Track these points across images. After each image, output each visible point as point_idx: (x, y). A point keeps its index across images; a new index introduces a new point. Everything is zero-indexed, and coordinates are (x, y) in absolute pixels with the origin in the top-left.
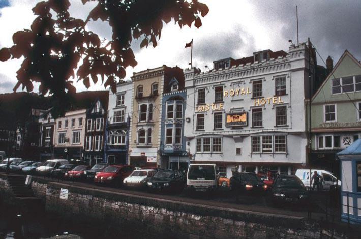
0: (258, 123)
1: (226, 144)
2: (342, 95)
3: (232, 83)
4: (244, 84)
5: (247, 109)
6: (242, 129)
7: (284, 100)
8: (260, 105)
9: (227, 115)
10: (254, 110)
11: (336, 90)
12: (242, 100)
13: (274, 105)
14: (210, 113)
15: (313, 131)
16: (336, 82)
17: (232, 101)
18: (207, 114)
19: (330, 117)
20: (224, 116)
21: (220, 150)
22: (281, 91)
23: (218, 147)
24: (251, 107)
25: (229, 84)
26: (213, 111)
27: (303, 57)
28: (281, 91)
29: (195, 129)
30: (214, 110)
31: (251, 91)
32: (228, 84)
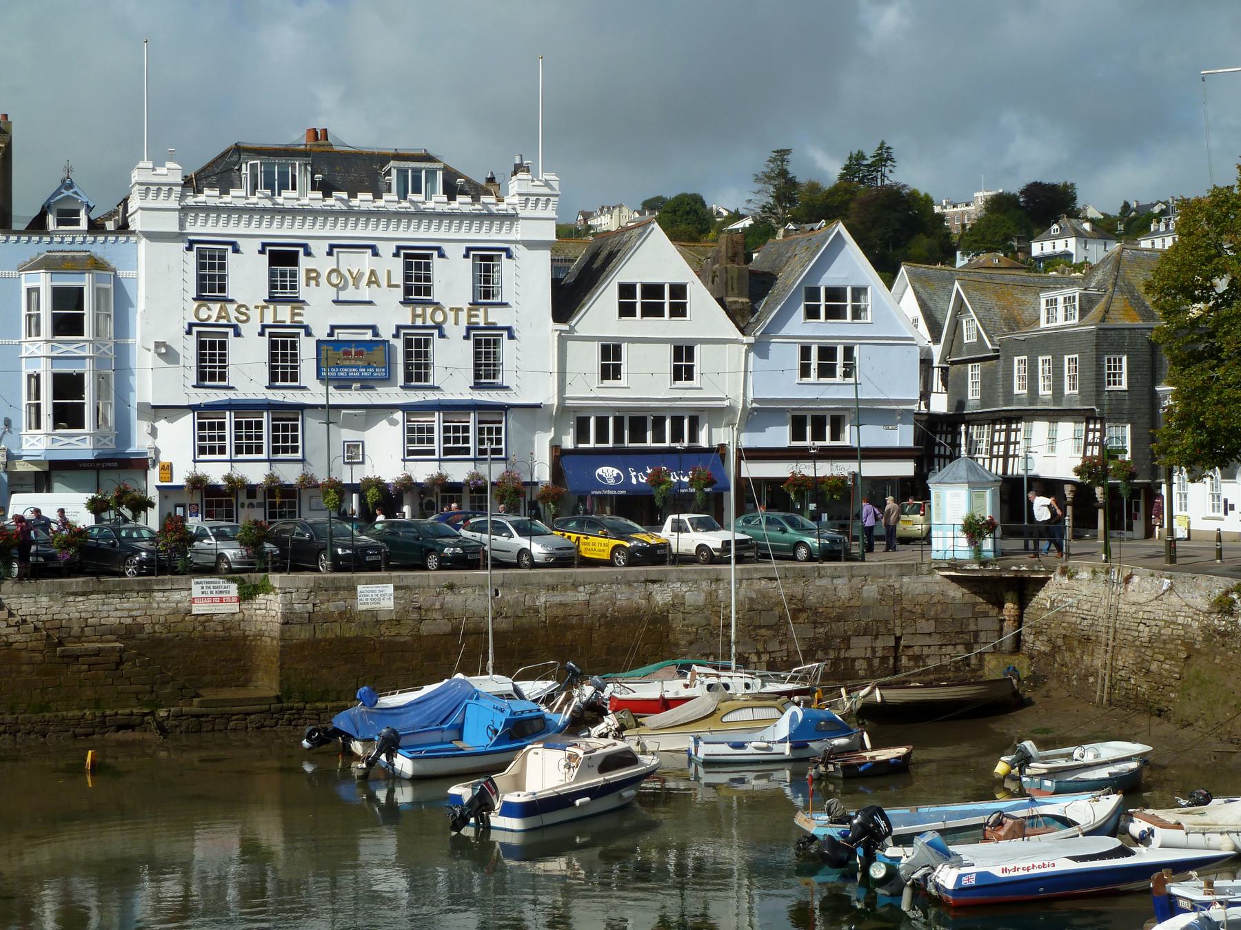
0: (418, 372)
1: (313, 428)
2: (639, 325)
3: (332, 247)
4: (375, 254)
5: (386, 333)
6: (372, 388)
7: (497, 316)
8: (429, 323)
9: (319, 342)
10: (408, 343)
11: (626, 310)
12: (370, 303)
13: (469, 329)
14: (250, 330)
15: (569, 403)
16: (626, 290)
17: (336, 302)
18: (238, 334)
19: (610, 371)
20: (307, 350)
21: (295, 450)
22: (485, 292)
23: (285, 442)
24: (399, 328)
25: (325, 246)
26: (264, 327)
27: (553, 215)
28: (485, 292)
29: (193, 379)
30: (269, 320)
31: (398, 278)
32: (320, 248)
